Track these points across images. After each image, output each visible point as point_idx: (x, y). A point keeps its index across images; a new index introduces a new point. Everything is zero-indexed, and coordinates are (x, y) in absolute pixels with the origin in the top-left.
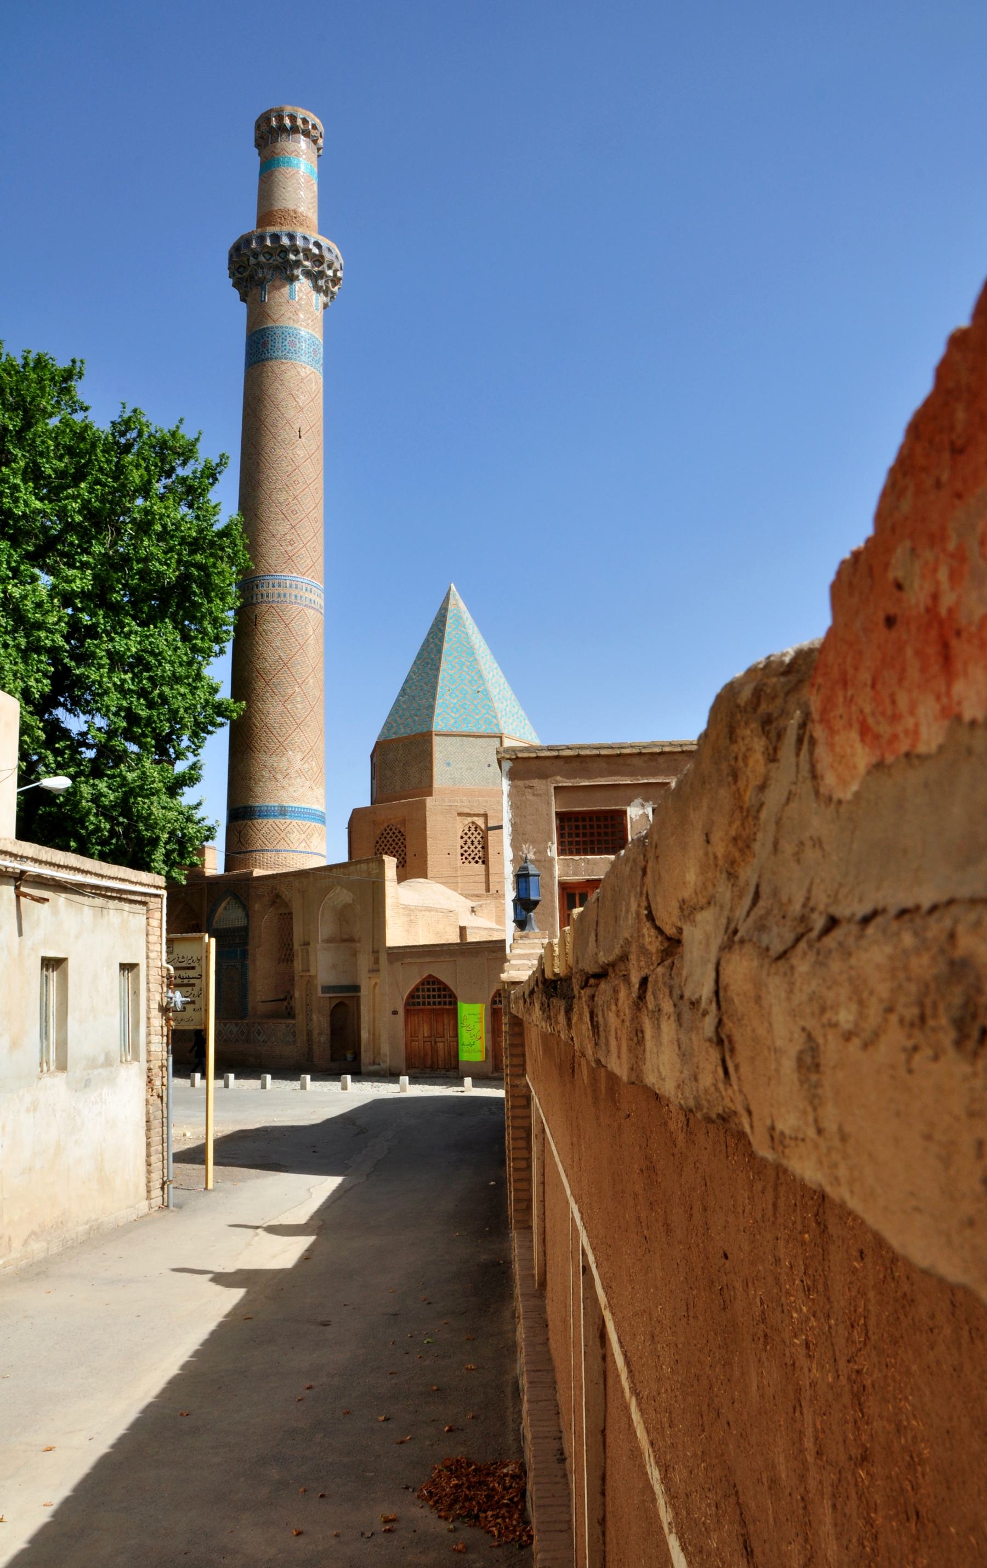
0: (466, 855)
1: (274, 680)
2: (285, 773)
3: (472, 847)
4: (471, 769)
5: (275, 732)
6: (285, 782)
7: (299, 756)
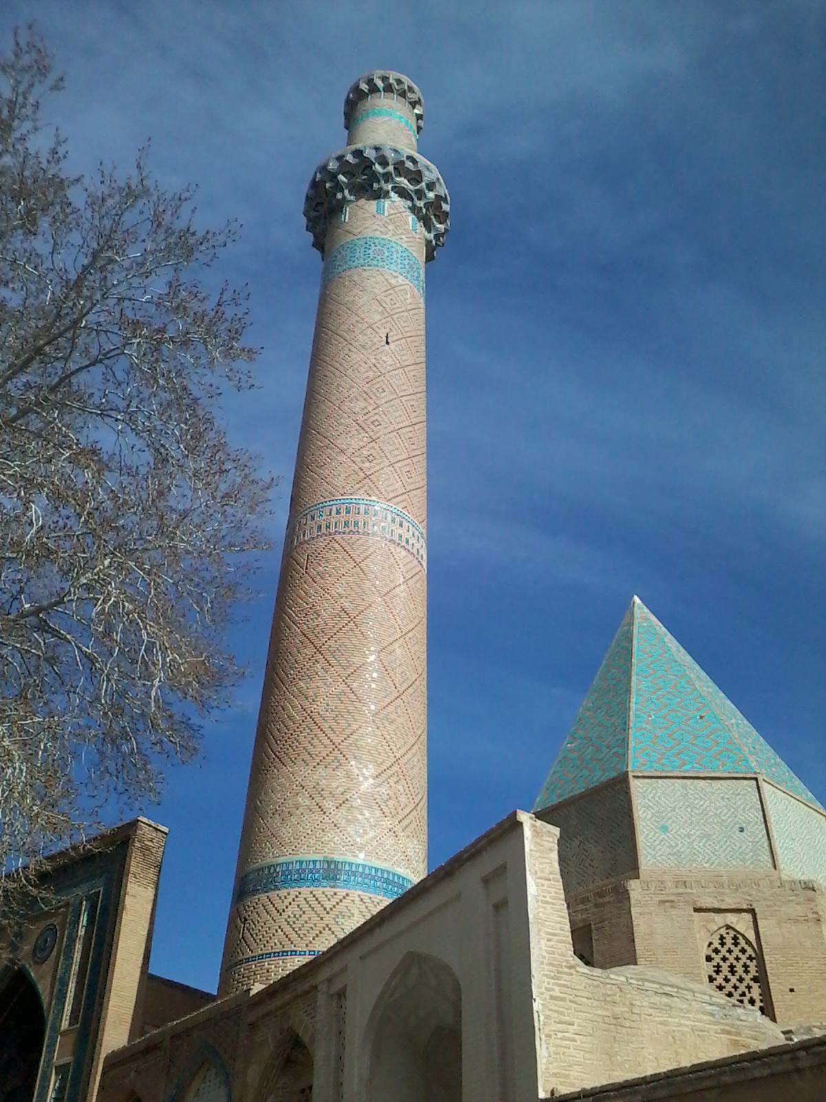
1: (331, 643)
2: (342, 798)
3: (734, 980)
5: (325, 726)
6: (340, 816)
7: (370, 770)
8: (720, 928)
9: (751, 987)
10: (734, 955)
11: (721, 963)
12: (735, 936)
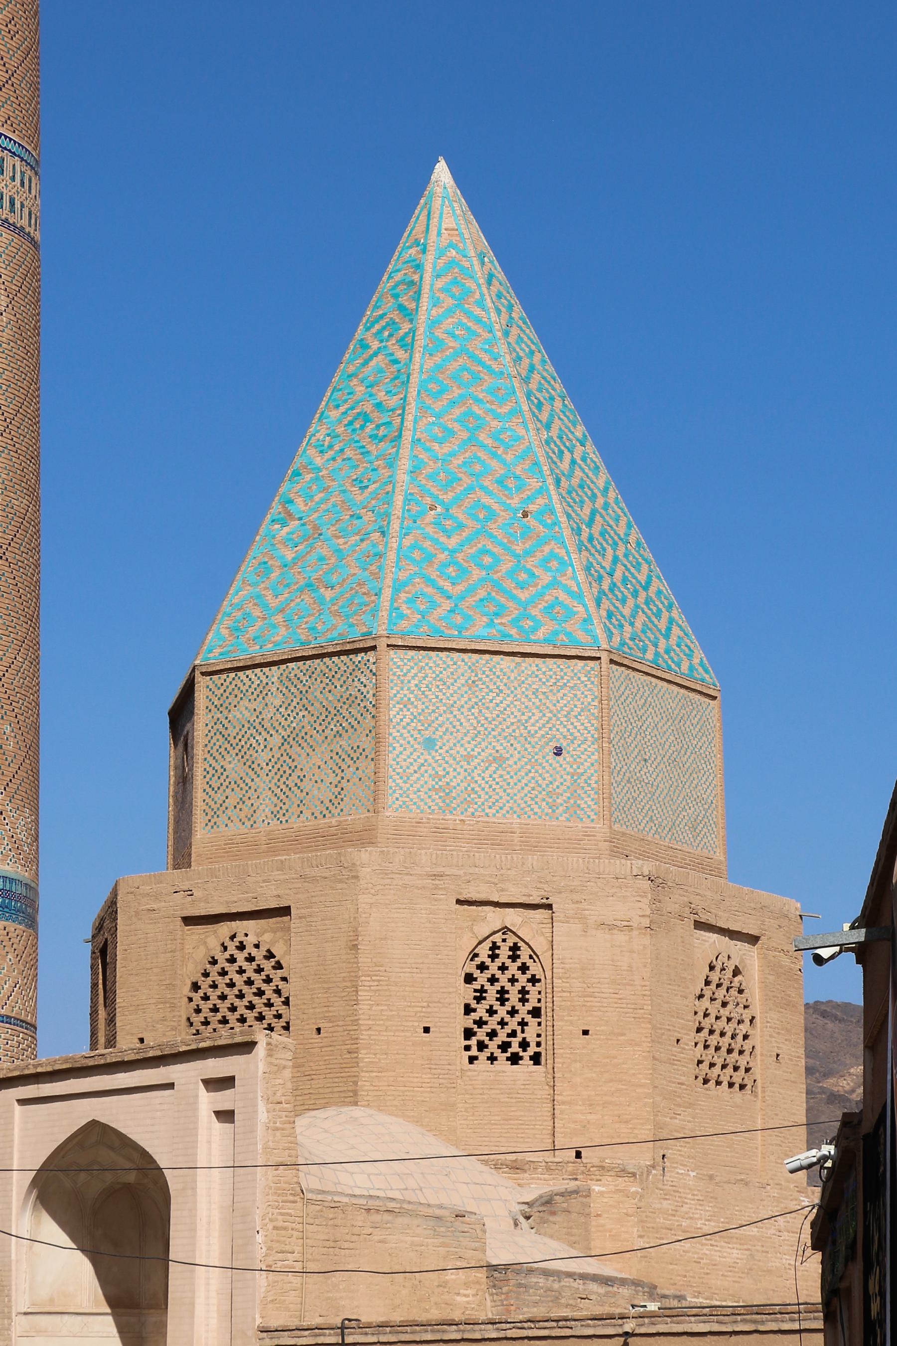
0: (481, 1034)
4: (500, 760)
8: (495, 933)
9: (526, 1024)
10: (508, 974)
11: (487, 986)
12: (515, 944)
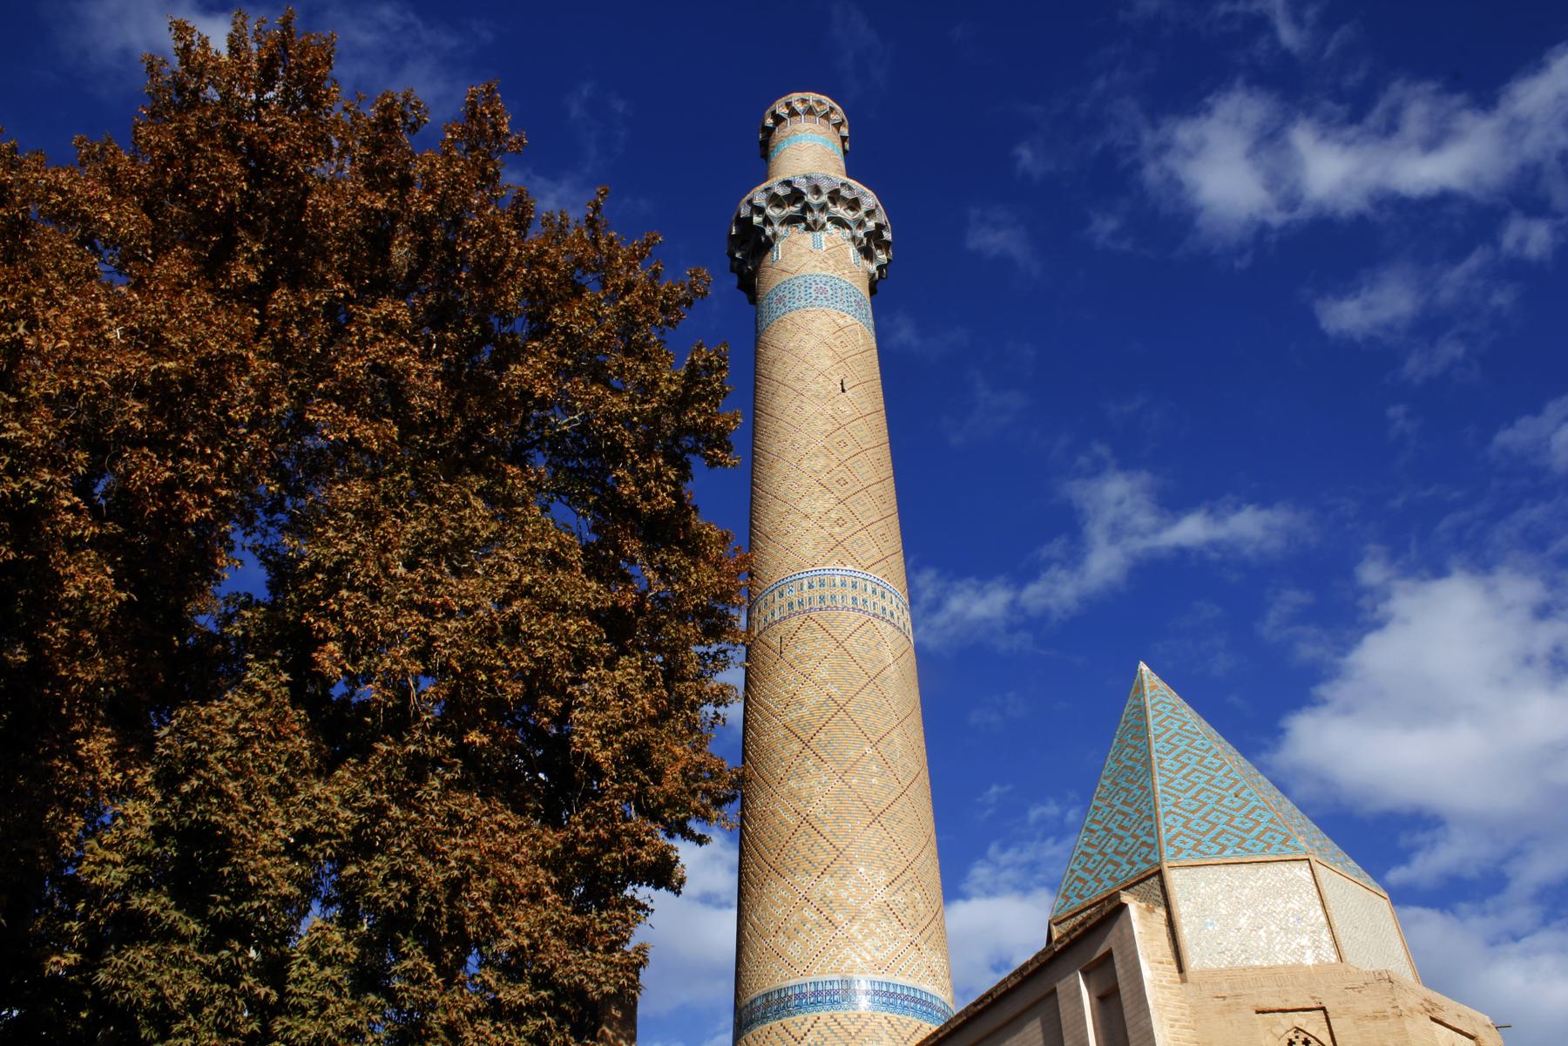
1: (821, 735)
5: (826, 830)
7: (883, 877)
